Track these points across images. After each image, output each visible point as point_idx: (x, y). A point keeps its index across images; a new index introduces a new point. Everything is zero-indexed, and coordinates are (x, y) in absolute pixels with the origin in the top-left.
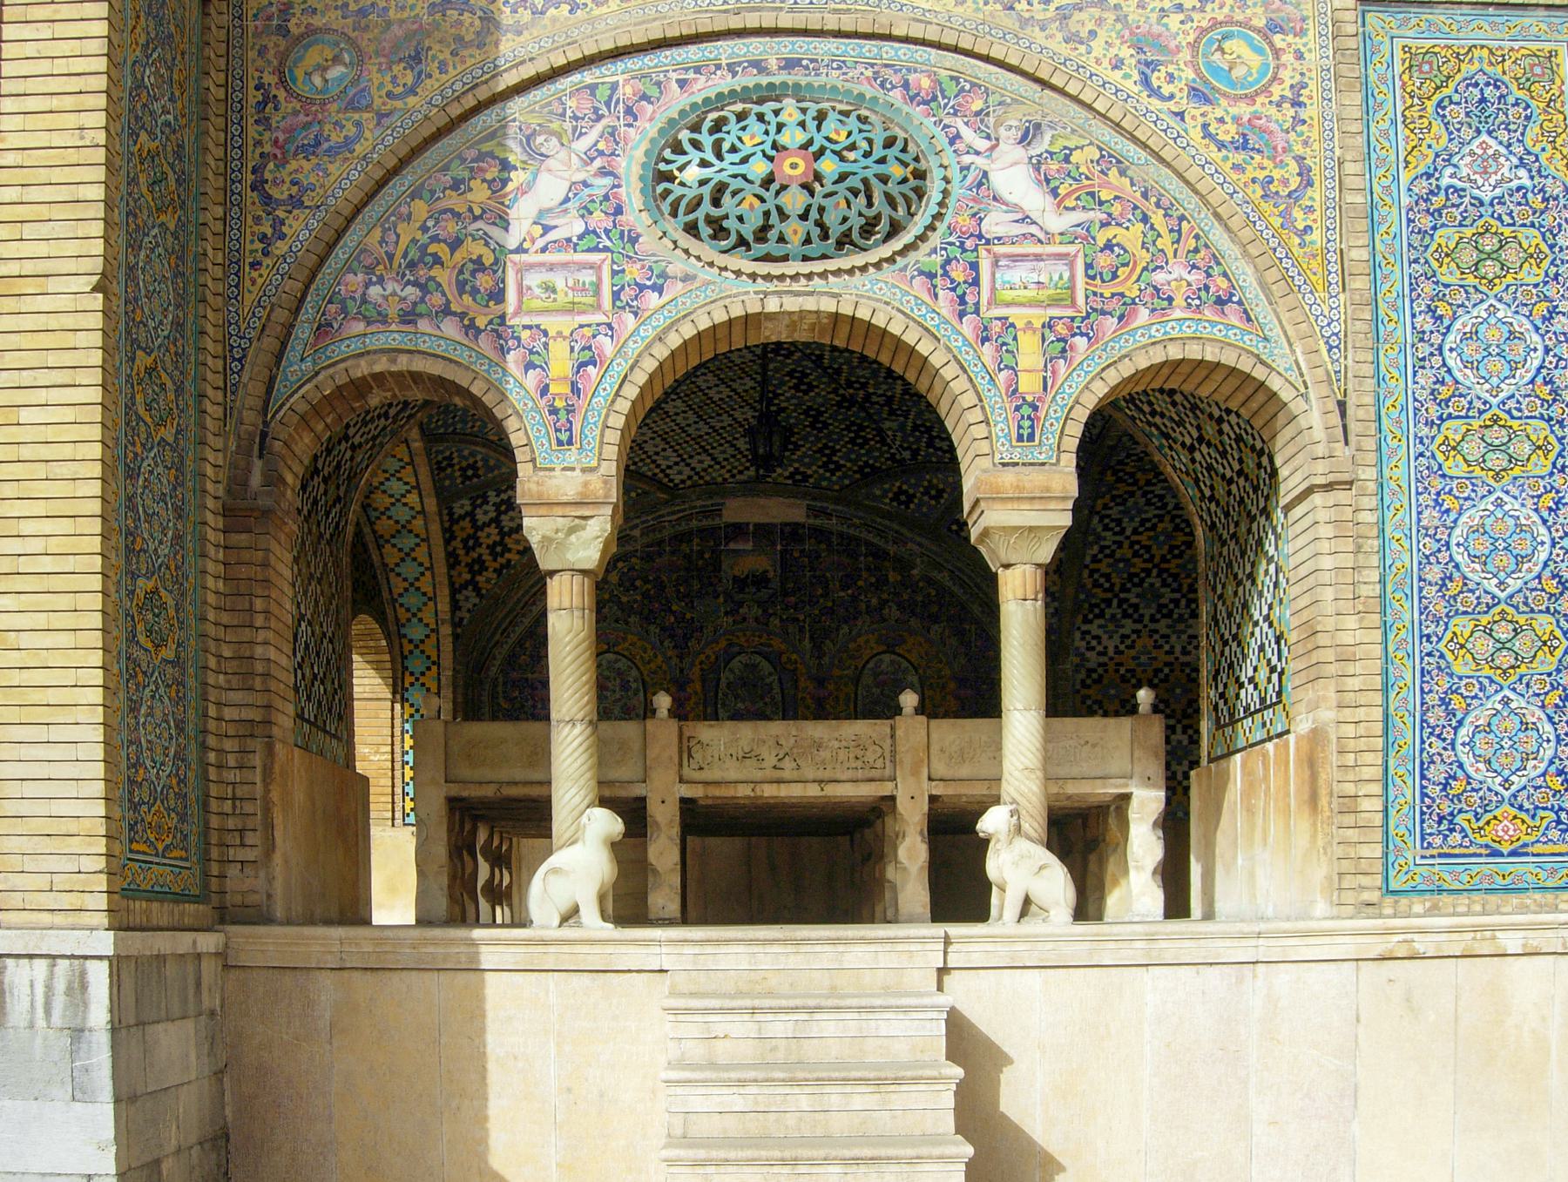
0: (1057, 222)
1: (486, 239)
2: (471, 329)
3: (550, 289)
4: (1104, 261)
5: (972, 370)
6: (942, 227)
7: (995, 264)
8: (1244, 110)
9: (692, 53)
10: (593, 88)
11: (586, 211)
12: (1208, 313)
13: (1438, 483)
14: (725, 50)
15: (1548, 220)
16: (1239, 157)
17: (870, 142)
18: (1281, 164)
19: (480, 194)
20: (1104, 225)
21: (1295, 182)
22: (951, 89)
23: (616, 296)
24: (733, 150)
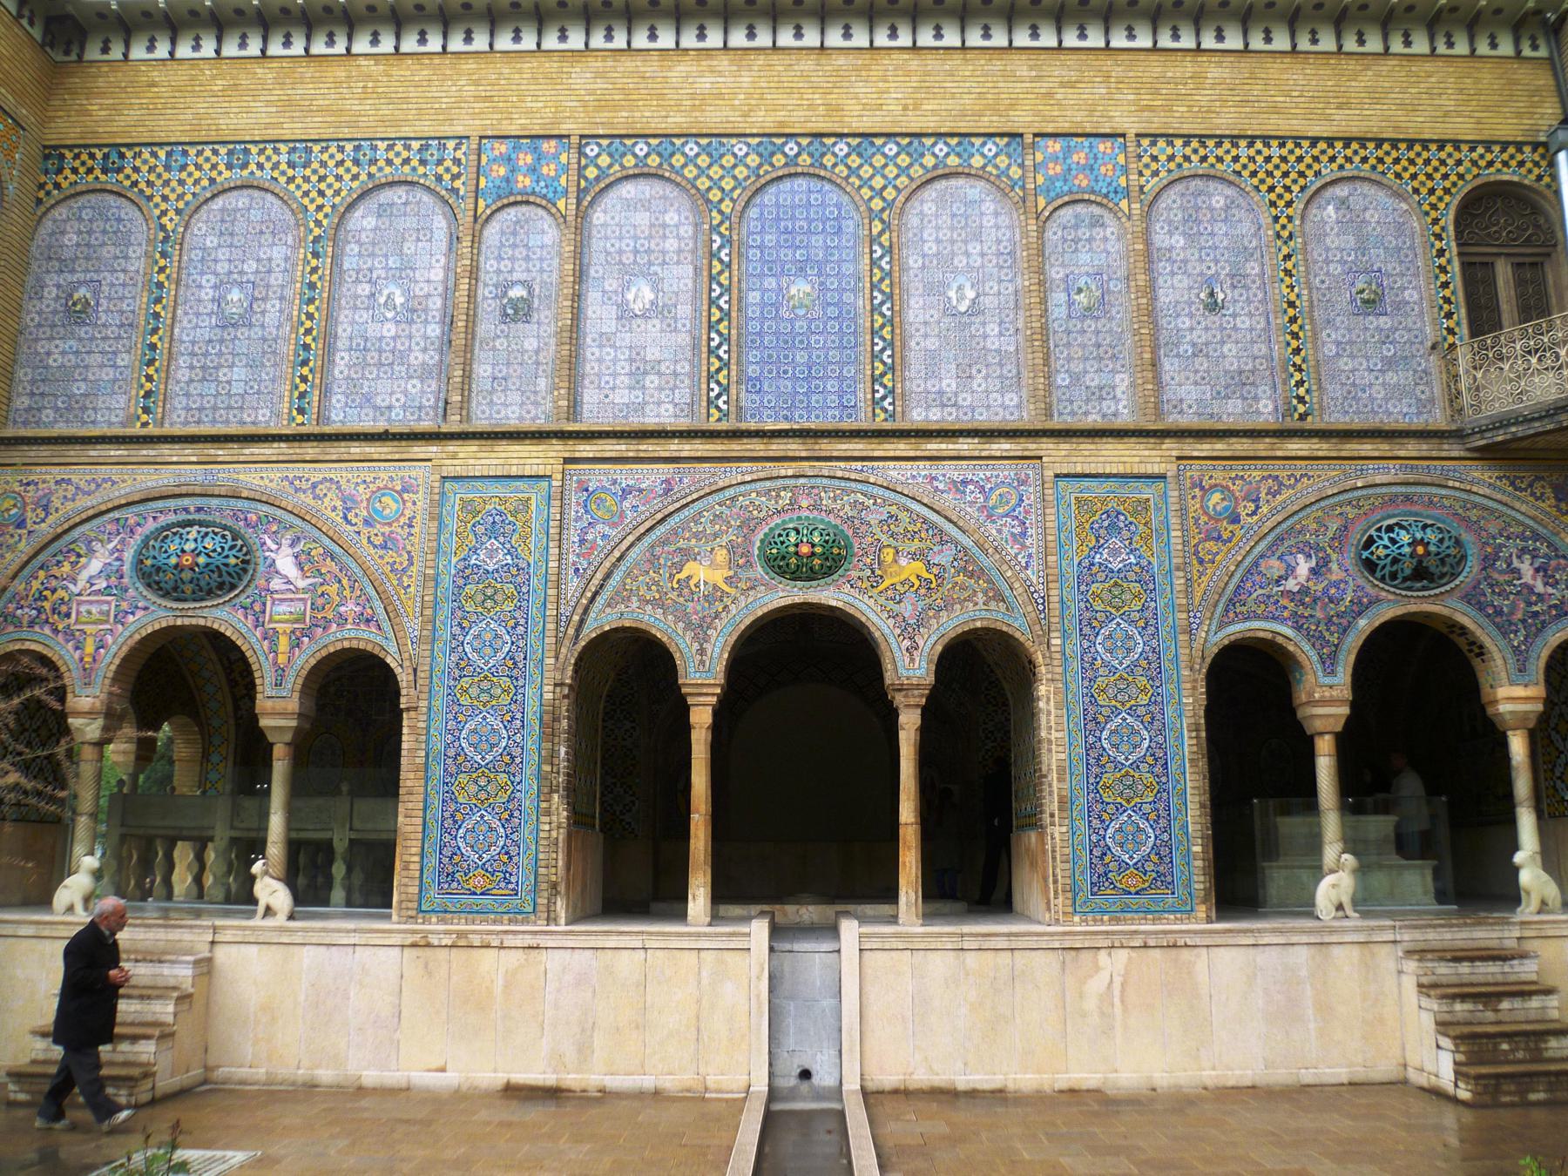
0: (301, 584)
1: (66, 588)
2: (56, 631)
3: (89, 612)
4: (320, 601)
5: (259, 653)
6: (253, 586)
7: (273, 604)
8: (387, 529)
9: (160, 504)
10: (118, 520)
11: (108, 577)
12: (362, 627)
13: (456, 708)
14: (172, 503)
15: (519, 579)
16: (381, 552)
17: (223, 548)
18: (401, 555)
19: (67, 567)
20: (322, 584)
21: (406, 563)
22: (264, 520)
23: (116, 616)
24: (166, 552)
